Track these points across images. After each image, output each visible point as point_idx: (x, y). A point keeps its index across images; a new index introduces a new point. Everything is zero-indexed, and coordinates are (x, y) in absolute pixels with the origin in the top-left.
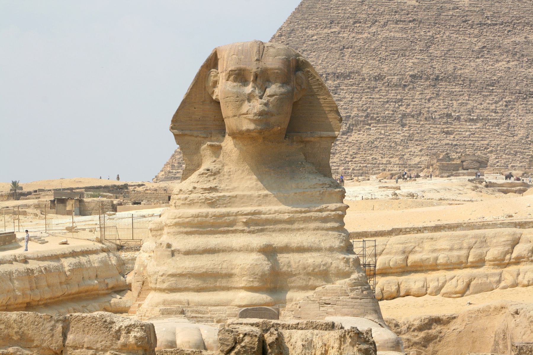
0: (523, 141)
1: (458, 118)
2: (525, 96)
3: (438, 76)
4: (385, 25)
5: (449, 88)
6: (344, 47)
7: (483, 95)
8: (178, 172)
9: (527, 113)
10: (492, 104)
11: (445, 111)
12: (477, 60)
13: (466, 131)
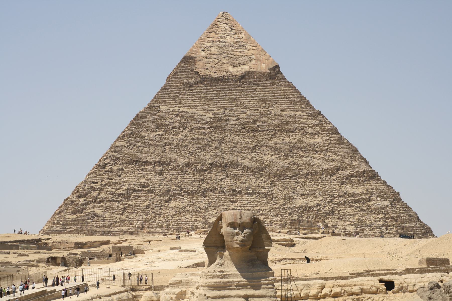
0: (282, 207)
1: (240, 192)
3: (227, 164)
4: (192, 130)
5: (234, 172)
6: (166, 145)
8: (57, 227)
11: (232, 187)
12: (252, 154)
13: (246, 201)
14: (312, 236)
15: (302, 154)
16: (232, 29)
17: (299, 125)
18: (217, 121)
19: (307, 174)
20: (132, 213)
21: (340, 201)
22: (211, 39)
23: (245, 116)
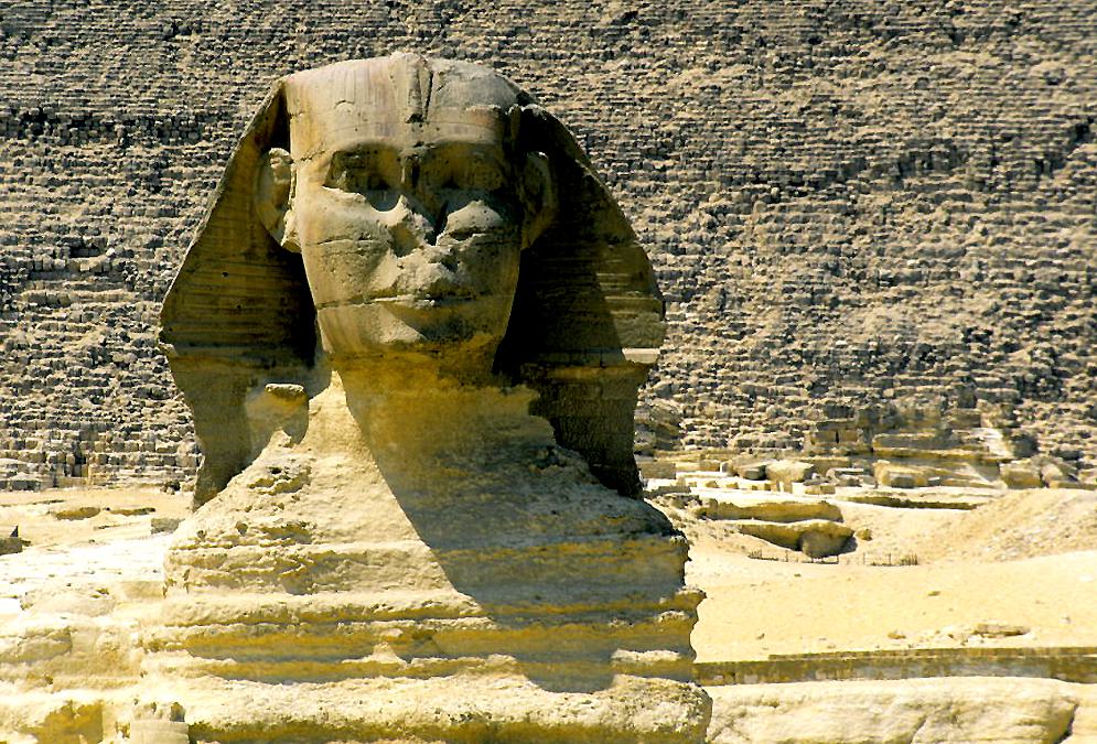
0: (774, 353)
2: (775, 190)
6: (176, 29)
7: (634, 190)
9: (783, 251)
10: (662, 221)
12: (609, 64)
14: (946, 493)
15: (873, 55)
19: (905, 167)
20: (27, 387)
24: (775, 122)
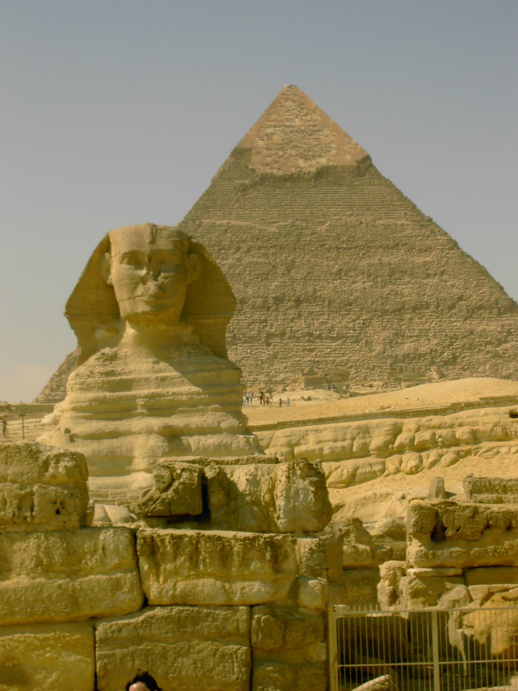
1: (319, 337)
3: (299, 298)
4: (249, 250)
8: (57, 395)
9: (383, 330)
10: (350, 322)
11: (307, 330)
12: (335, 282)
13: (327, 348)
16: (302, 108)
17: (401, 239)
18: (285, 237)
21: (464, 344)
22: (273, 123)
23: (323, 228)
24: (381, 297)
